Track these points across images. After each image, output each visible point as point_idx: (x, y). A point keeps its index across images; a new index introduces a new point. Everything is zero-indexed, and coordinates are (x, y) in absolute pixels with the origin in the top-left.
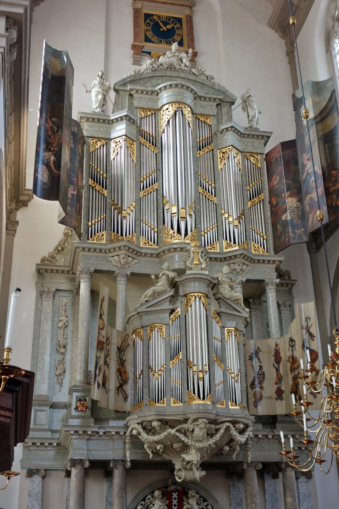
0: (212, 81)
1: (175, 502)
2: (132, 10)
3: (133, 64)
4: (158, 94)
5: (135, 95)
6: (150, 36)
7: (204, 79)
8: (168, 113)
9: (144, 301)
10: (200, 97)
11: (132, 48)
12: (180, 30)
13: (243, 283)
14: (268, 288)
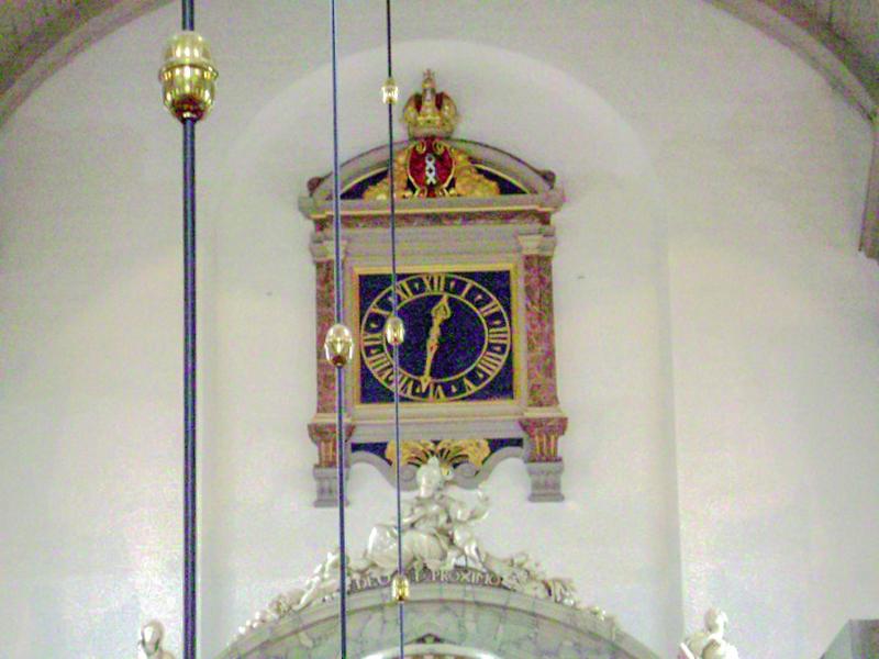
0: (566, 601)
2: (313, 269)
6: (381, 373)
7: (536, 597)
11: (311, 435)
12: (503, 324)
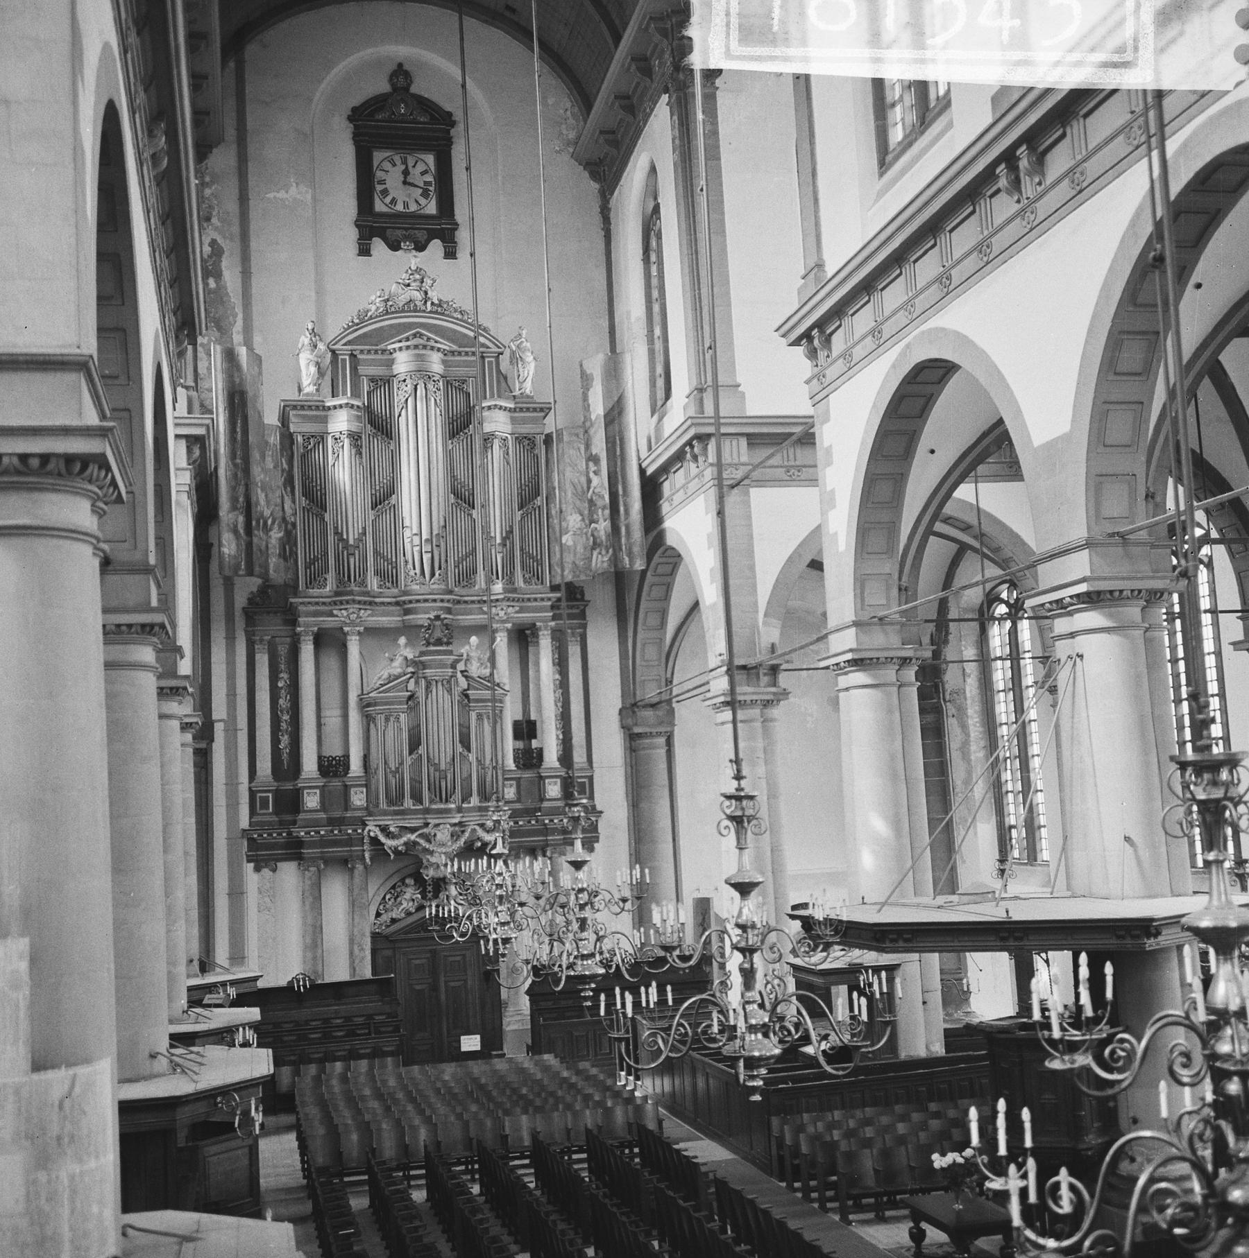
1: (430, 888)
3: (359, 255)
4: (391, 353)
5: (360, 356)
8: (406, 389)
9: (377, 685)
10: (453, 353)
13: (508, 630)
14: (541, 633)
